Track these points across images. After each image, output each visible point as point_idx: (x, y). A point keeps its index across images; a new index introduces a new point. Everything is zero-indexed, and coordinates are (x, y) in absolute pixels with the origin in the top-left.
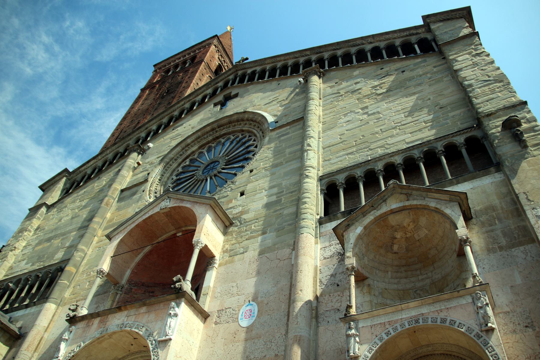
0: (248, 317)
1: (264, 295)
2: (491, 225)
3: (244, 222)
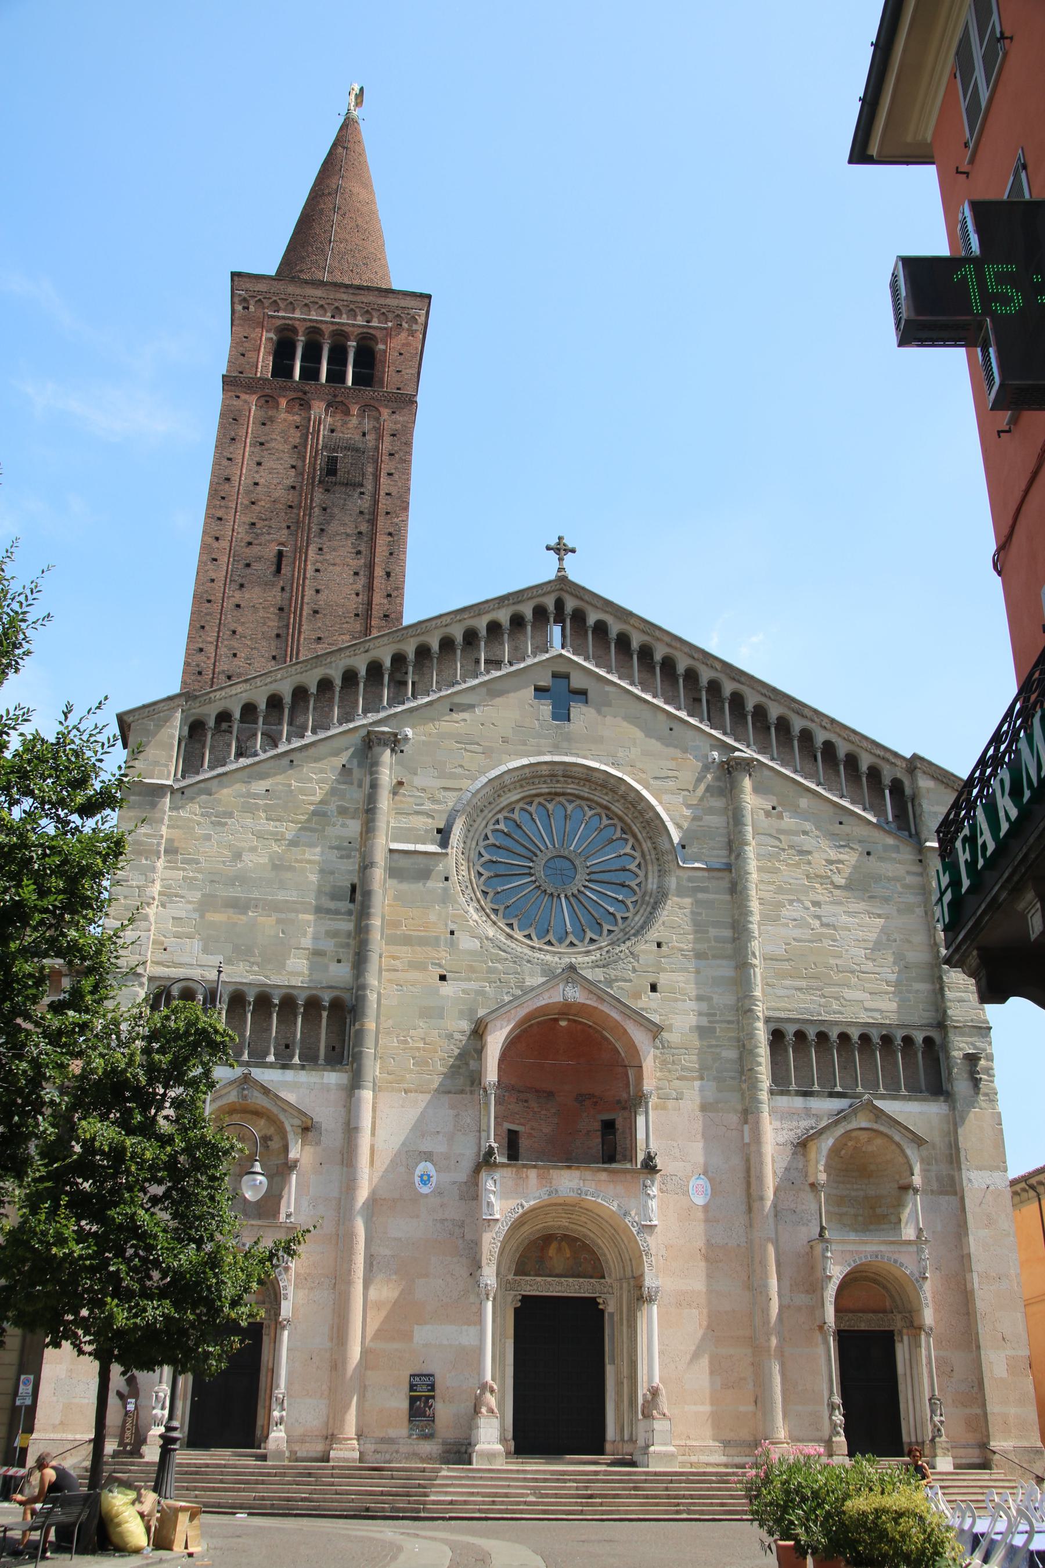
2: (928, 1164)
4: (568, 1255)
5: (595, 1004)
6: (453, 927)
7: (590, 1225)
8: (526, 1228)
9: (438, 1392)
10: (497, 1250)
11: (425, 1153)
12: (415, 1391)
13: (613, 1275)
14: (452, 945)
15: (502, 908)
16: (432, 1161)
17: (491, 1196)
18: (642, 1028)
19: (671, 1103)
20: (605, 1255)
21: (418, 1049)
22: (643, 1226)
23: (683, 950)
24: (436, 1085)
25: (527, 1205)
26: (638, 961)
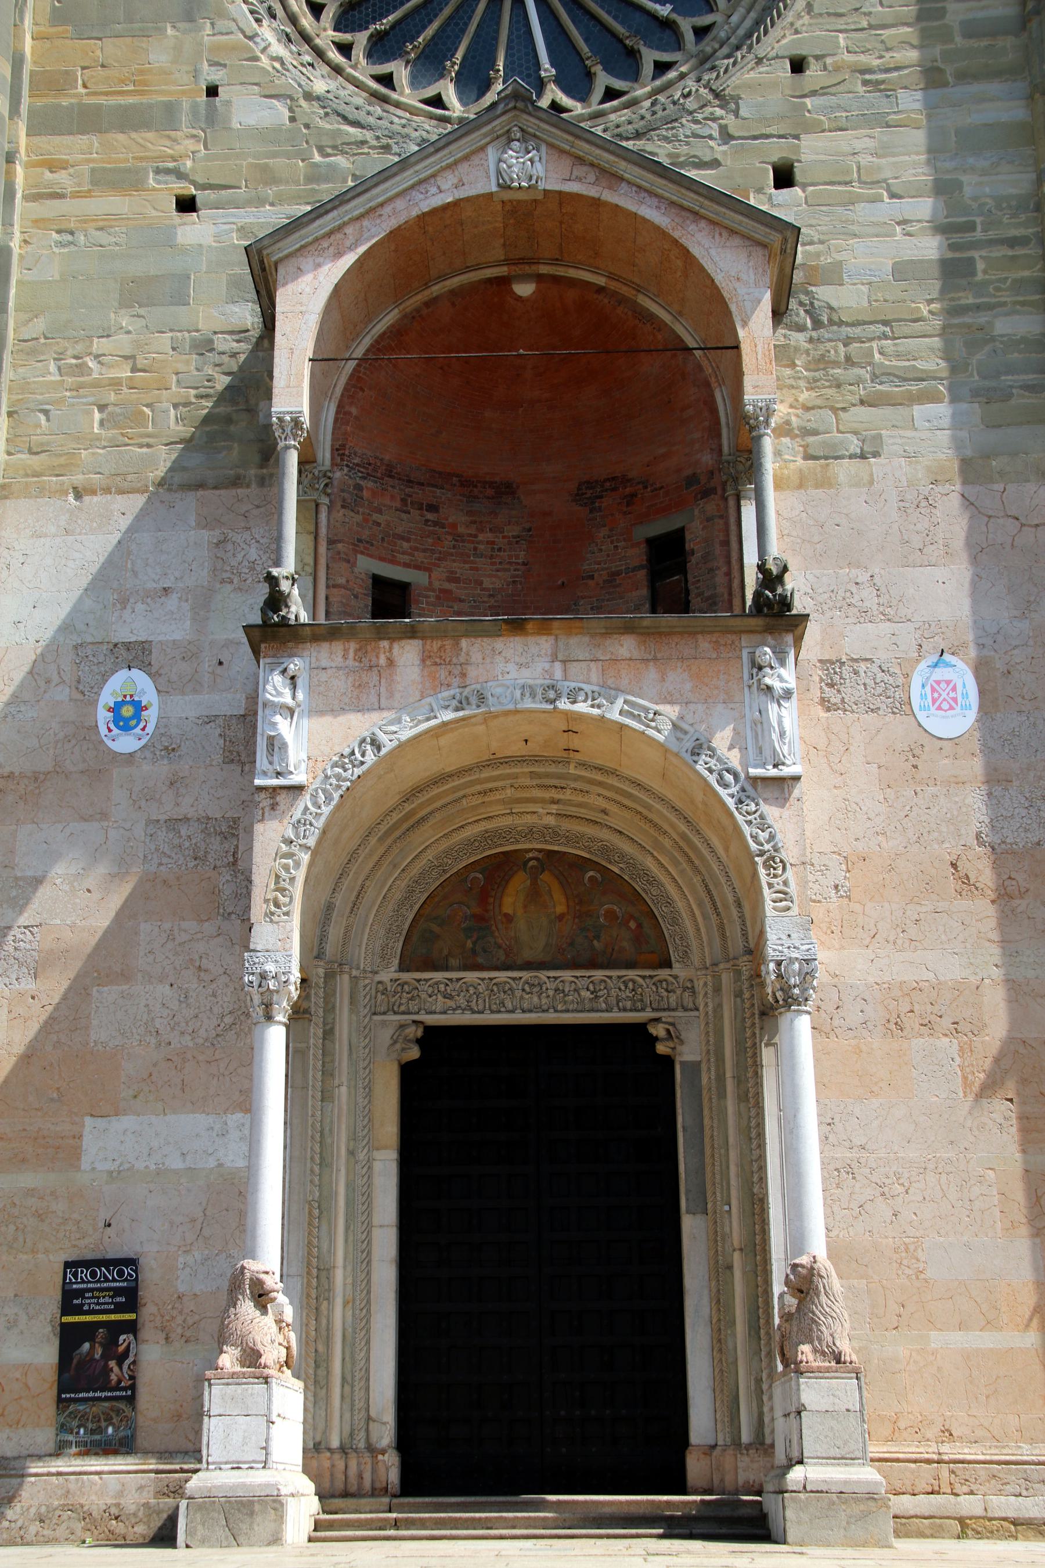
0: (945, 706)
1: (988, 641)
3: (831, 322)
4: (561, 909)
5: (592, 192)
6: (215, 76)
7: (618, 818)
8: (426, 835)
9: (149, 1311)
10: (301, 875)
11: (128, 646)
12: (79, 1310)
13: (696, 959)
14: (212, 119)
15: (361, 40)
16: (146, 667)
17: (278, 718)
18: (737, 241)
19: (844, 470)
20: (670, 902)
21: (115, 384)
22: (755, 780)
23: (870, 71)
24: (160, 473)
25: (388, 745)
26: (737, 115)
